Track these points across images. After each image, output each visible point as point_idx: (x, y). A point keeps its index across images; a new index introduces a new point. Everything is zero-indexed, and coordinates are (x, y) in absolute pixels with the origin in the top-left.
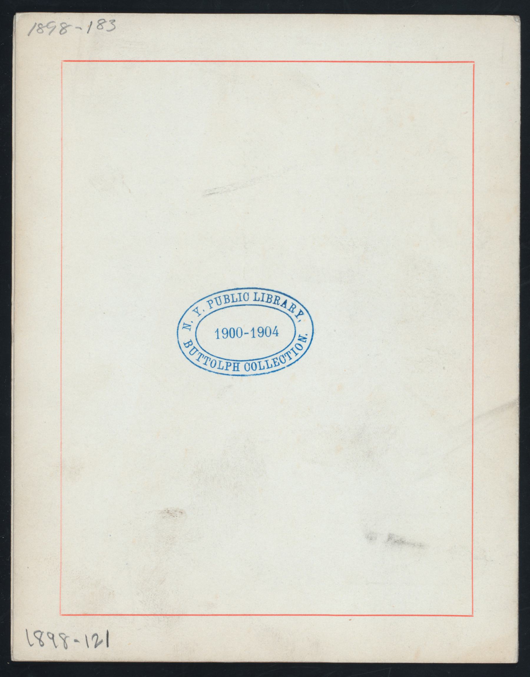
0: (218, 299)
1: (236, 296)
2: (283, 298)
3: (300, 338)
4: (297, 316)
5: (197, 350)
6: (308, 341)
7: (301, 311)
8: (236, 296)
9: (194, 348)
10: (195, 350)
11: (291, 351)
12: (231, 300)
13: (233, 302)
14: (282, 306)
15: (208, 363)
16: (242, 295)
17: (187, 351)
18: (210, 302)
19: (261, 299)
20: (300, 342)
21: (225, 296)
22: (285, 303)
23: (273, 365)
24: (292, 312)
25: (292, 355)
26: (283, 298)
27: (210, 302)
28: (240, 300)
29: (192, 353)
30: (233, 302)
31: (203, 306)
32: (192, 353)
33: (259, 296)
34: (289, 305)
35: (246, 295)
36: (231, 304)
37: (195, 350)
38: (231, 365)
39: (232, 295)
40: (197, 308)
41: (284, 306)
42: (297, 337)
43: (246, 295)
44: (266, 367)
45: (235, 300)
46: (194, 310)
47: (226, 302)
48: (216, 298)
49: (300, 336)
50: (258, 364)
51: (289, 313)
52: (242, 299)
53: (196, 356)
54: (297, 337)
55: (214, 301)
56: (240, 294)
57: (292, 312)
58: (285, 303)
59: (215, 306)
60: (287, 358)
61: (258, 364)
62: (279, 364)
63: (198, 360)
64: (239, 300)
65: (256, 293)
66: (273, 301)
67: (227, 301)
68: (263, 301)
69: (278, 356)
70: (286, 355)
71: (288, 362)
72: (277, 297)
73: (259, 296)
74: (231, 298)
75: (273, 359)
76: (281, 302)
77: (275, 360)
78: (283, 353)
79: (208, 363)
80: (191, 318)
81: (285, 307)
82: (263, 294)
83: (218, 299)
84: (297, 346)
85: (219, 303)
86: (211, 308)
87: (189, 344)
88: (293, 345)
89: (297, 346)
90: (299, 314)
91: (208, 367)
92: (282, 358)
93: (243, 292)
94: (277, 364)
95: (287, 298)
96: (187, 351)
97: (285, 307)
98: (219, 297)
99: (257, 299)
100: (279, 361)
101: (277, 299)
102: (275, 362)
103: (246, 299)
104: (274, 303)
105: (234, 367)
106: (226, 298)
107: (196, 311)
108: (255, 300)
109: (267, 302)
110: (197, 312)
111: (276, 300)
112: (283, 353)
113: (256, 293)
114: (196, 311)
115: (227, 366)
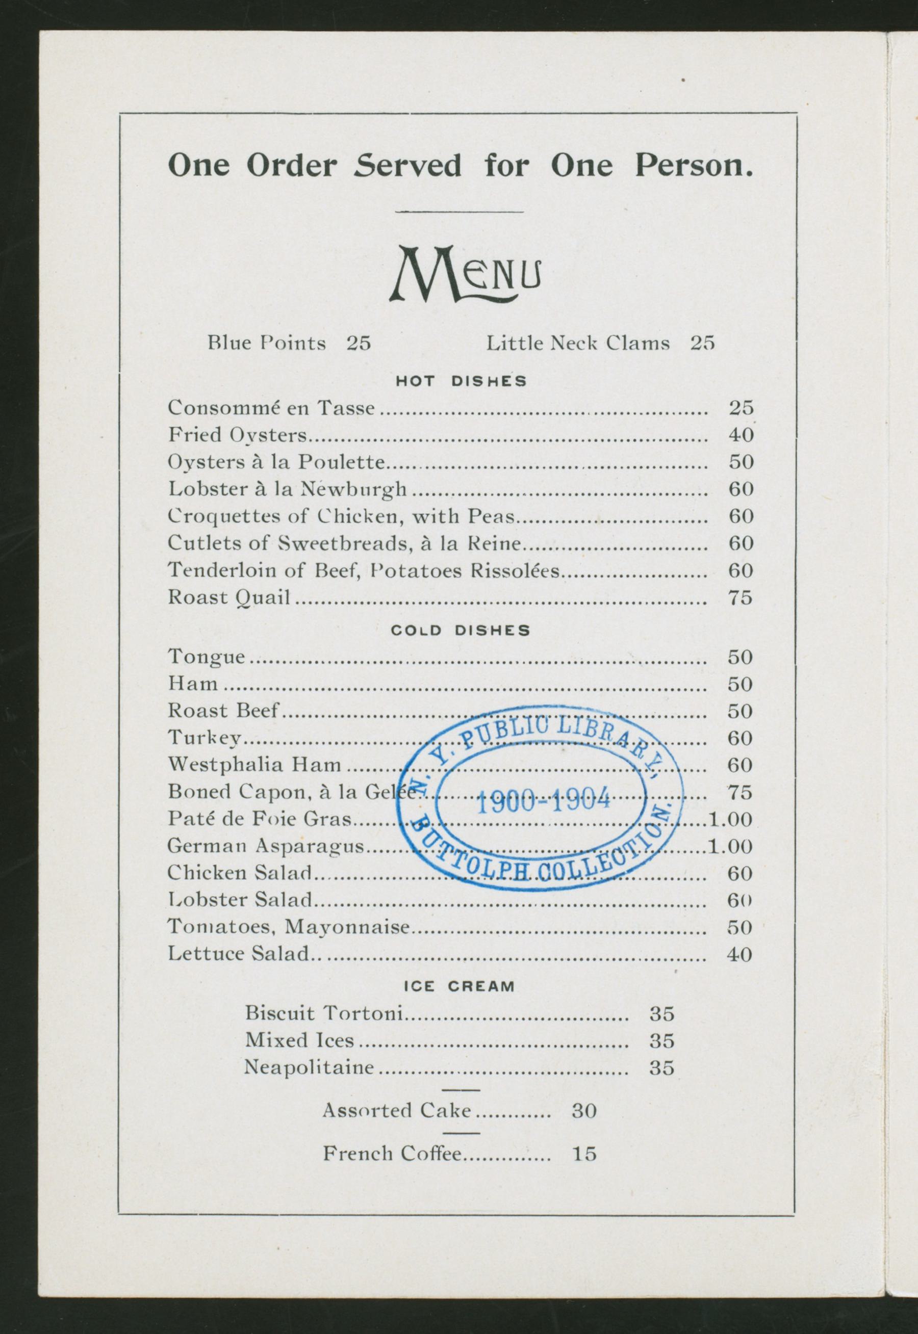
0: (483, 729)
2: (620, 728)
3: (656, 811)
5: (439, 837)
10: (434, 836)
11: (637, 840)
12: (511, 732)
13: (515, 734)
15: (463, 863)
17: (417, 838)
18: (467, 736)
20: (656, 821)
23: (600, 868)
24: (640, 757)
26: (620, 728)
28: (530, 732)
29: (428, 842)
30: (515, 734)
32: (428, 842)
37: (434, 836)
38: (510, 868)
45: (518, 731)
46: (433, 753)
48: (478, 728)
50: (567, 867)
52: (534, 728)
54: (649, 810)
55: (475, 733)
57: (640, 757)
61: (567, 867)
62: (611, 867)
64: (526, 730)
67: (503, 732)
68: (577, 733)
74: (509, 726)
77: (604, 858)
79: (463, 863)
83: (483, 729)
92: (617, 854)
94: (607, 866)
96: (417, 838)
98: (486, 725)
99: (565, 728)
100: (610, 859)
101: (608, 729)
102: (602, 863)
105: (518, 872)
108: (561, 731)
110: (440, 757)
111: (605, 730)
115: (502, 870)
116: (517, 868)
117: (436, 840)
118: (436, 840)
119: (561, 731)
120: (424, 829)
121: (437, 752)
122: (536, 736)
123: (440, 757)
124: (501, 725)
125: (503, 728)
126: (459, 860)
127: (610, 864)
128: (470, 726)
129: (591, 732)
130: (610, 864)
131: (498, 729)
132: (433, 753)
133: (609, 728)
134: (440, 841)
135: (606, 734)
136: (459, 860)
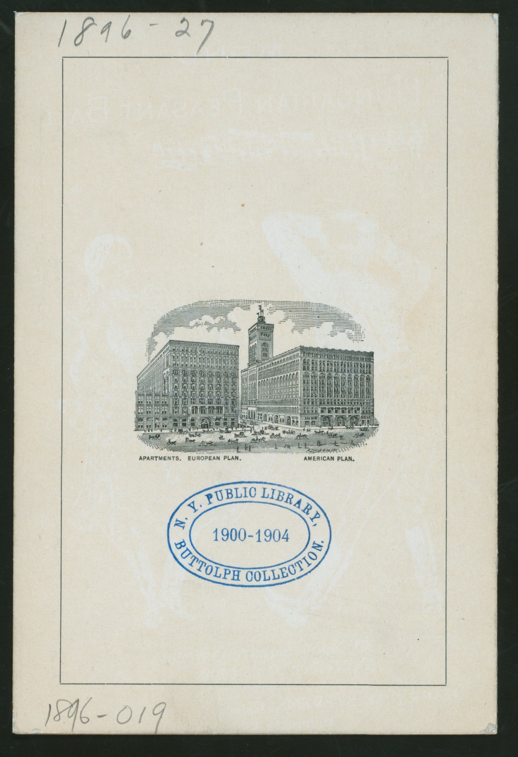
0: (219, 493)
1: (241, 491)
2: (297, 497)
3: (315, 545)
4: (312, 519)
5: (191, 553)
6: (324, 549)
7: (317, 513)
8: (241, 491)
9: (187, 549)
10: (188, 552)
11: (303, 561)
12: (235, 496)
13: (237, 497)
14: (295, 505)
15: (203, 569)
16: (248, 490)
19: (270, 496)
20: (314, 551)
21: (227, 490)
22: (299, 502)
23: (281, 576)
24: (307, 513)
25: (304, 565)
26: (297, 497)
27: (209, 496)
28: (245, 496)
29: (184, 556)
30: (237, 497)
31: (201, 500)
32: (184, 556)
33: (269, 492)
34: (303, 505)
35: (253, 490)
36: (234, 500)
37: (188, 552)
39: (236, 489)
40: (193, 502)
41: (297, 505)
42: (311, 544)
43: (253, 490)
44: (272, 577)
45: (239, 495)
46: (189, 505)
47: (228, 498)
48: (216, 492)
49: (314, 543)
50: (262, 574)
51: (304, 515)
52: (248, 494)
53: (189, 560)
54: (311, 544)
55: (214, 495)
56: (245, 488)
57: (307, 513)
58: (299, 502)
60: (298, 568)
61: (262, 574)
62: (287, 576)
63: (191, 565)
64: (243, 495)
66: (285, 499)
67: (230, 496)
68: (272, 498)
69: (286, 565)
70: (297, 564)
71: (299, 573)
72: (289, 494)
73: (269, 492)
74: (234, 492)
75: (281, 569)
76: (294, 501)
77: (284, 570)
78: (293, 562)
79: (203, 569)
82: (274, 490)
83: (219, 493)
84: (311, 555)
85: (220, 498)
86: (210, 503)
87: (181, 545)
88: (305, 554)
89: (311, 555)
90: (315, 517)
91: (202, 574)
92: (291, 568)
93: (249, 486)
94: (285, 575)
95: (300, 497)
96: (178, 553)
97: (299, 507)
98: (220, 491)
99: (266, 496)
100: (287, 571)
102: (283, 573)
103: (253, 495)
104: (286, 502)
105: (234, 575)
106: (229, 493)
107: (192, 506)
108: (263, 497)
110: (193, 508)
111: (288, 498)
112: (293, 562)
115: (225, 574)
116: (234, 573)
117: (189, 554)
118: (189, 554)
120: (182, 548)
121: (192, 505)
122: (249, 499)
123: (193, 508)
124: (229, 491)
125: (230, 493)
126: (201, 567)
127: (287, 574)
128: (211, 492)
129: (280, 498)
130: (287, 574)
131: (228, 494)
132: (189, 505)
133: (290, 497)
134: (191, 555)
135: (289, 500)
136: (201, 567)
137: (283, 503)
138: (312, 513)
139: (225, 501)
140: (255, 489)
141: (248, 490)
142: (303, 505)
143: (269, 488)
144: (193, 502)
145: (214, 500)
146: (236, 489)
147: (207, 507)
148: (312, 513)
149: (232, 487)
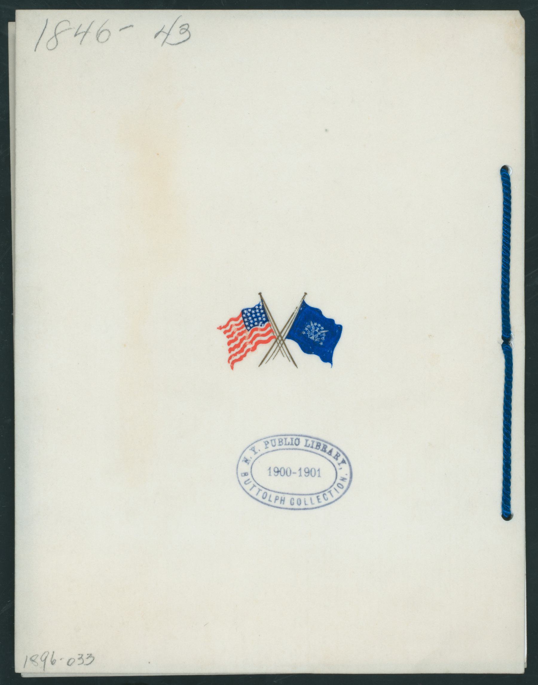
0: (273, 441)
8: (289, 440)
14: (328, 453)
16: (294, 440)
22: (331, 451)
24: (337, 459)
27: (267, 443)
30: (286, 444)
34: (334, 453)
35: (297, 441)
39: (286, 439)
48: (271, 440)
55: (270, 442)
57: (337, 459)
58: (331, 451)
59: (271, 448)
64: (290, 443)
65: (307, 441)
68: (312, 447)
73: (310, 442)
76: (328, 450)
80: (249, 454)
81: (330, 455)
83: (273, 441)
99: (308, 445)
101: (325, 447)
106: (280, 441)
107: (253, 450)
108: (306, 446)
109: (316, 448)
110: (254, 451)
113: (307, 441)
114: (253, 450)
119: (306, 446)
131: (279, 442)
137: (319, 452)
138: (340, 459)
139: (277, 447)
140: (299, 440)
141: (294, 440)
142: (334, 453)
143: (310, 440)
144: (254, 448)
145: (270, 445)
146: (286, 439)
147: (263, 450)
148: (340, 459)
149: (283, 437)
